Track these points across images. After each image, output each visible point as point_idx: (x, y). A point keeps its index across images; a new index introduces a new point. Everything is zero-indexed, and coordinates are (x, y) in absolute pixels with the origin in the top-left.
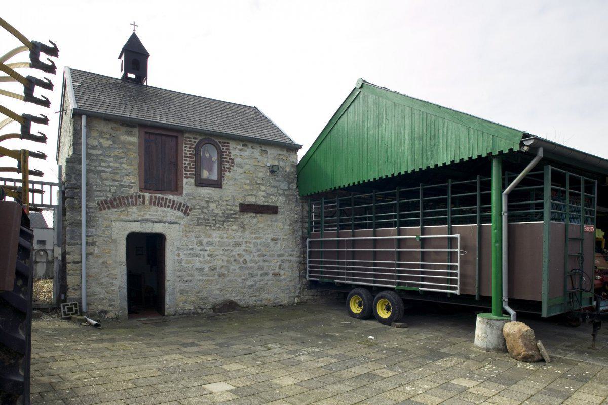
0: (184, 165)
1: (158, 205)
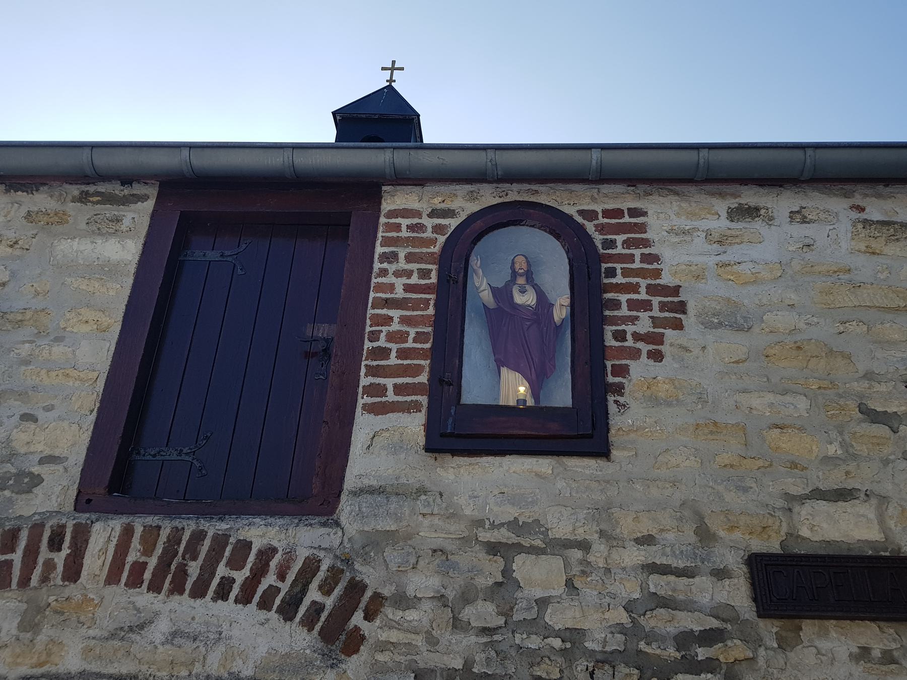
1: (155, 587)
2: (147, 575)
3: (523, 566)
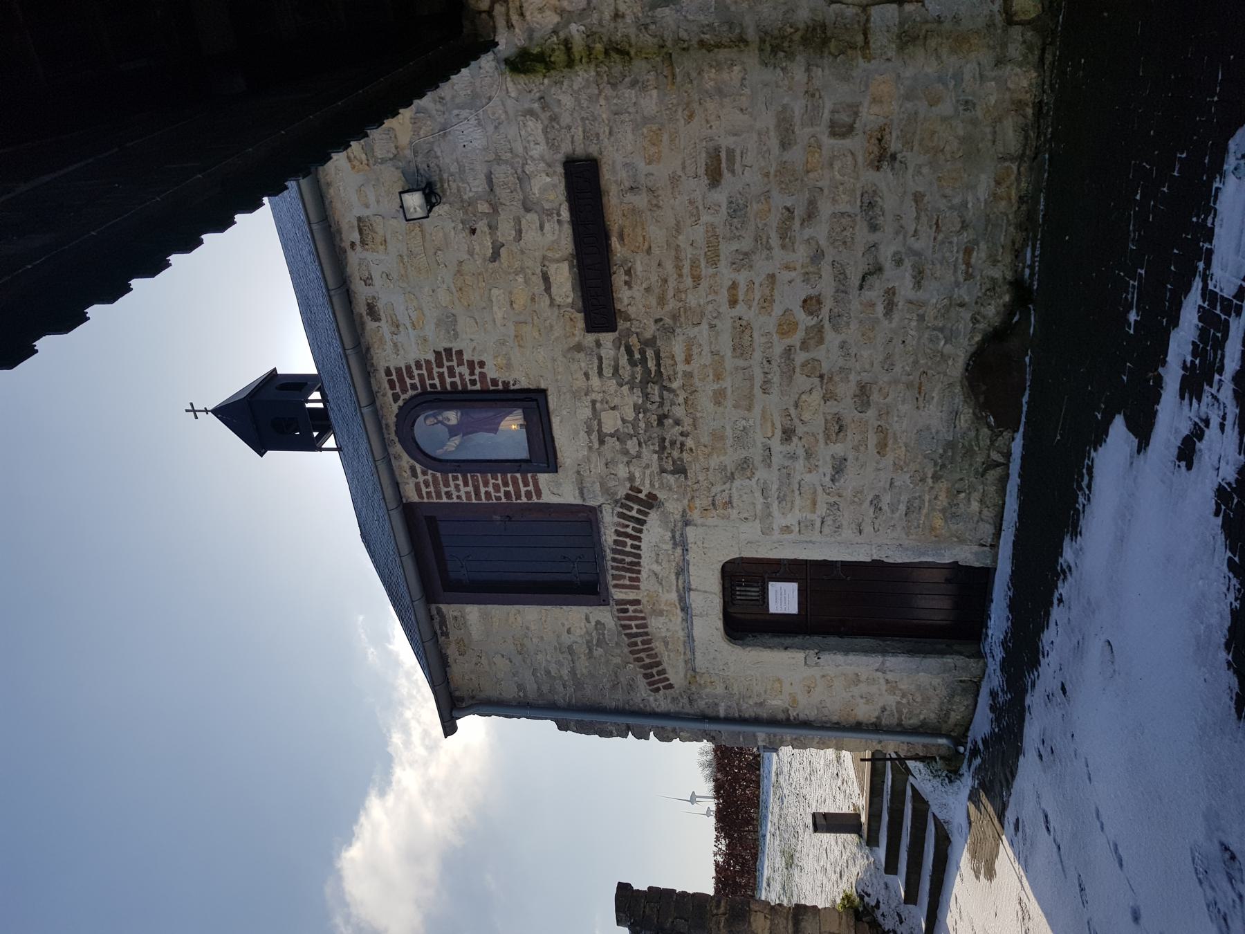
0: (504, 500)
1: (639, 572)
2: (634, 575)
3: (608, 428)
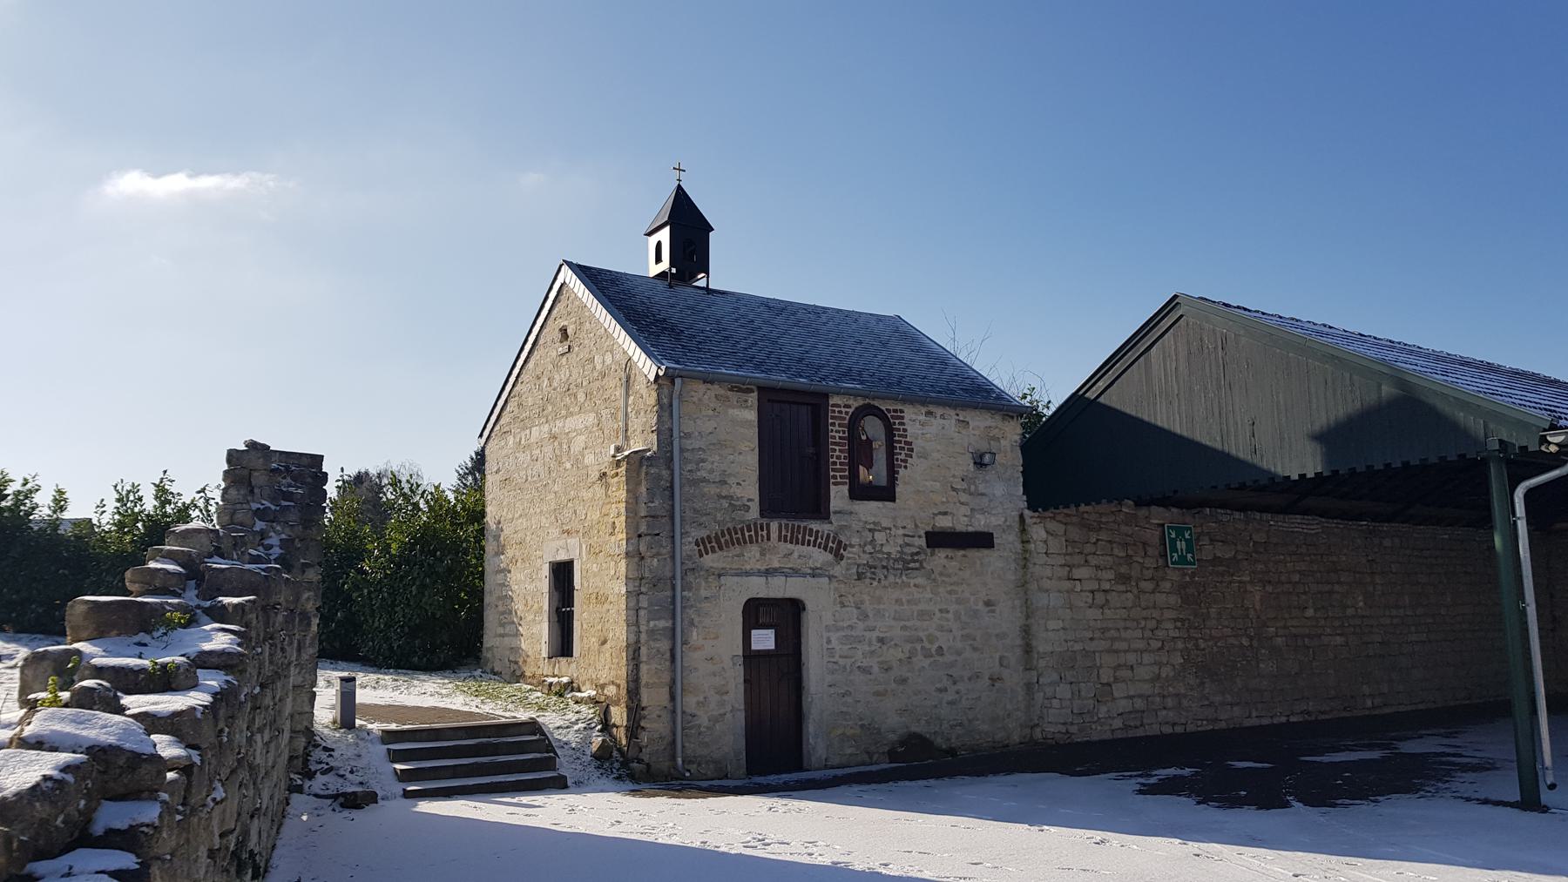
1: (791, 543)
2: (788, 539)
3: (877, 534)
